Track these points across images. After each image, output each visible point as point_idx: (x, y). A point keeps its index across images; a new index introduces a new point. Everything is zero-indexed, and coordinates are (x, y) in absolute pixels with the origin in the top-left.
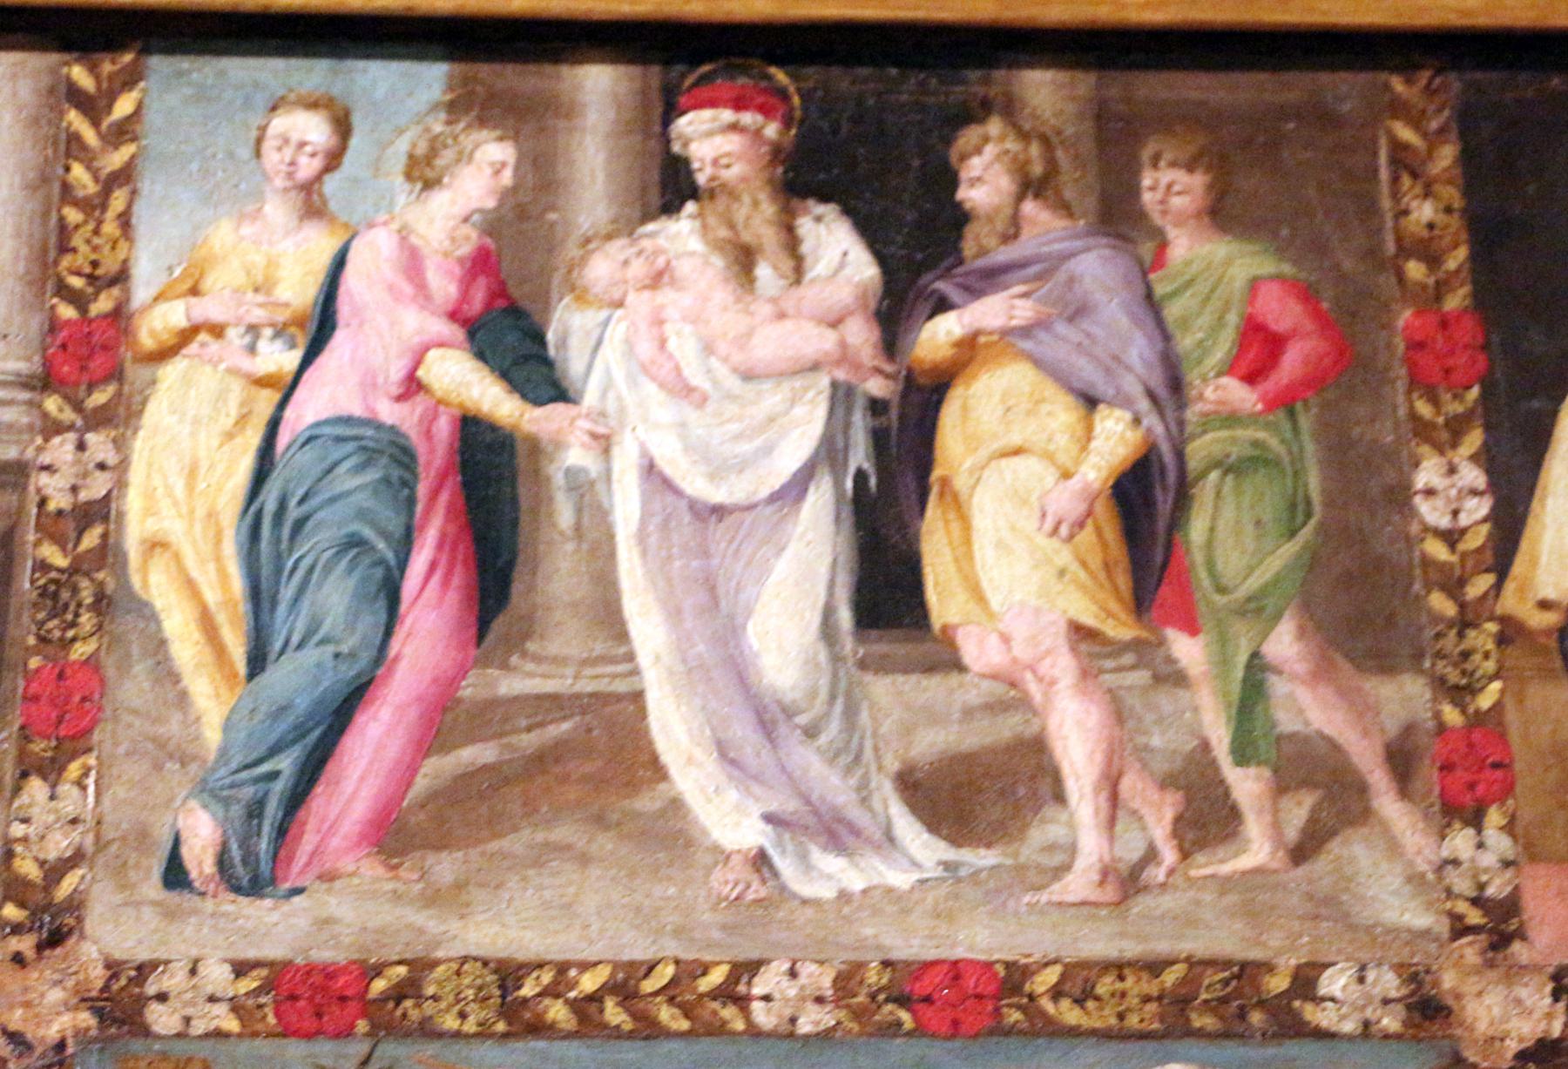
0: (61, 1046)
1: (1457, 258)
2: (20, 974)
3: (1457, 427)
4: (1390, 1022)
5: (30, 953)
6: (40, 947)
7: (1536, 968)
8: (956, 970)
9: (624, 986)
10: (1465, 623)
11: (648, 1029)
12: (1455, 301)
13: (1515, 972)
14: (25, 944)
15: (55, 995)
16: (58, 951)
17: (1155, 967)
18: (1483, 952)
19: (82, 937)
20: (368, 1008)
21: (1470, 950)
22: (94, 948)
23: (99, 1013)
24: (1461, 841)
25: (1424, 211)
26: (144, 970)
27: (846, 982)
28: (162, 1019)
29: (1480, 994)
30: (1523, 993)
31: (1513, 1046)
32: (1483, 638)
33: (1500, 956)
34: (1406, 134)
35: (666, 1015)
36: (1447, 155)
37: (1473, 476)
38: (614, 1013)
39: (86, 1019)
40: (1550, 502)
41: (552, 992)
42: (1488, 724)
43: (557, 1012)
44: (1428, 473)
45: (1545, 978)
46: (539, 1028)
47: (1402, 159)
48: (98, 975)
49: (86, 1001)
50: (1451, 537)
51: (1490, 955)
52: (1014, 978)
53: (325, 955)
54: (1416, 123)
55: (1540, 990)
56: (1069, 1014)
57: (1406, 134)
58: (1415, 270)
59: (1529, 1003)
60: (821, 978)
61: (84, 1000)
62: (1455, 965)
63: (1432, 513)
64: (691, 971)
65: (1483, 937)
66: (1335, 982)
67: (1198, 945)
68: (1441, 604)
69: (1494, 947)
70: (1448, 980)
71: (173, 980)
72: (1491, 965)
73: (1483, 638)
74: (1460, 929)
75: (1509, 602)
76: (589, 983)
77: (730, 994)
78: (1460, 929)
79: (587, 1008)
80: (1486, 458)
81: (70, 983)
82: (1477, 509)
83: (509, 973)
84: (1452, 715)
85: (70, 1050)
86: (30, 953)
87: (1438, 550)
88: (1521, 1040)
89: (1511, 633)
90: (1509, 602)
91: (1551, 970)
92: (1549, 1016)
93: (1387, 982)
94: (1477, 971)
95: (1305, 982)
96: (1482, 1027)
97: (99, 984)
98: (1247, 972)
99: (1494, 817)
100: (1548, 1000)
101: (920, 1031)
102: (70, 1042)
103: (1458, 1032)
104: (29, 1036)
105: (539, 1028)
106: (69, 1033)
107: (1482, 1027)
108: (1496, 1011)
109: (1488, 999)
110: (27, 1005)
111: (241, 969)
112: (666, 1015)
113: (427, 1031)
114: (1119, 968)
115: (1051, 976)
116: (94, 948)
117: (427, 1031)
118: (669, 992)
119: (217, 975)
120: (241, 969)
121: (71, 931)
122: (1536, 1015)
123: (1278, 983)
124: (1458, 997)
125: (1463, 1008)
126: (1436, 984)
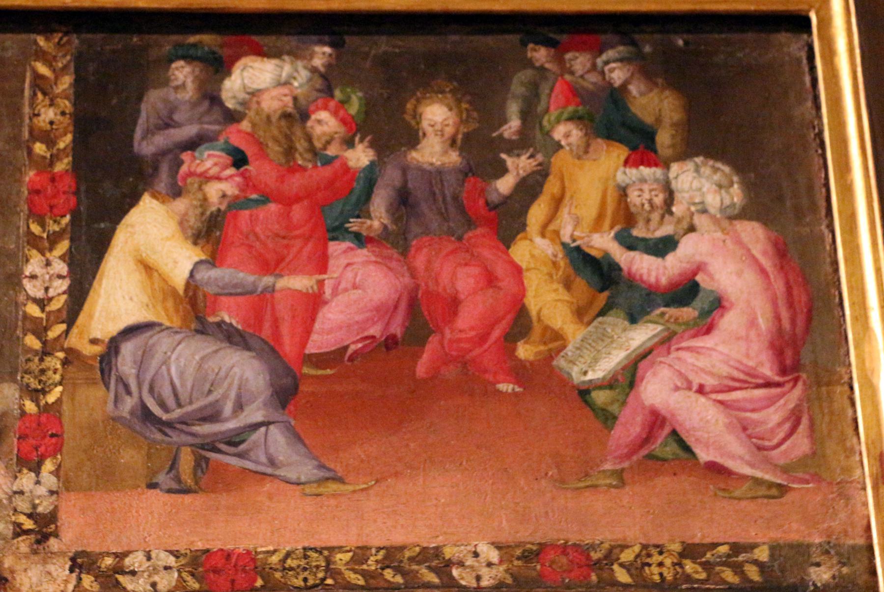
1: (65, 141)
3: (54, 240)
7: (62, 554)
10: (45, 353)
12: (61, 166)
21: (23, 545)
24: (26, 480)
25: (48, 114)
29: (25, 570)
30: (51, 568)
32: (54, 362)
33: (41, 547)
34: (42, 69)
36: (66, 81)
37: (61, 267)
40: (104, 282)
42: (52, 411)
44: (34, 265)
45: (67, 559)
47: (40, 84)
50: (41, 303)
51: (35, 546)
54: (49, 64)
55: (62, 567)
57: (42, 69)
58: (39, 148)
59: (54, 574)
62: (13, 553)
63: (33, 289)
65: (32, 537)
68: (32, 342)
69: (38, 542)
72: (35, 552)
73: (54, 362)
74: (19, 531)
75: (73, 341)
78: (19, 531)
80: (69, 258)
82: (62, 285)
84: (30, 407)
87: (33, 310)
89: (72, 358)
90: (73, 341)
91: (71, 554)
94: (26, 557)
99: (48, 466)
100: (67, 572)
108: (34, 580)
109: (30, 574)
122: (59, 581)
124: (12, 572)
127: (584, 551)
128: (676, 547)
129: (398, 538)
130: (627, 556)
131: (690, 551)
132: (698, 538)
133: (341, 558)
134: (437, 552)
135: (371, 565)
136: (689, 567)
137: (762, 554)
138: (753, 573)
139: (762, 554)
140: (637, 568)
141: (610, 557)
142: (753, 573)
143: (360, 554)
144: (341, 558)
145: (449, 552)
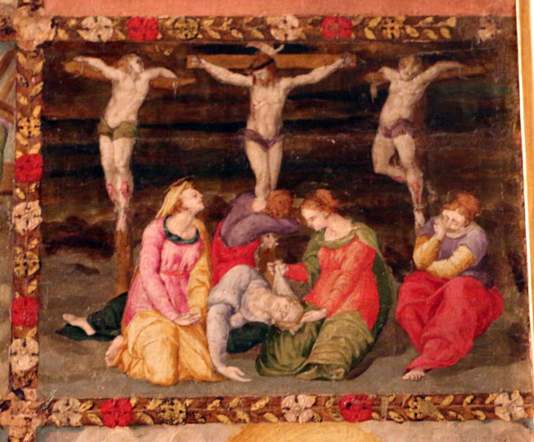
7: (46, 17)
13: (39, 19)
18: (29, 12)
21: (24, 11)
29: (26, 26)
31: (36, 43)
33: (34, 13)
45: (49, 20)
51: (31, 13)
59: (42, 29)
62: (18, 16)
65: (29, 7)
70: (16, 21)
72: (31, 16)
88: (39, 41)
91: (51, 18)
92: (49, 33)
94: (26, 18)
96: (26, 37)
100: (49, 28)
103: (17, 39)
107: (26, 37)
108: (31, 32)
109: (28, 28)
122: (45, 33)
124: (19, 27)
125: (19, 30)
126: (11, 22)
127: (347, 20)
128: (402, 18)
129: (240, 12)
130: (373, 24)
131: (410, 21)
132: (415, 14)
133: (207, 23)
134: (263, 20)
135: (225, 27)
136: (409, 30)
137: (452, 23)
138: (446, 34)
139: (452, 23)
140: (378, 30)
141: (363, 24)
142: (446, 34)
143: (218, 21)
144: (207, 23)
145: (270, 20)
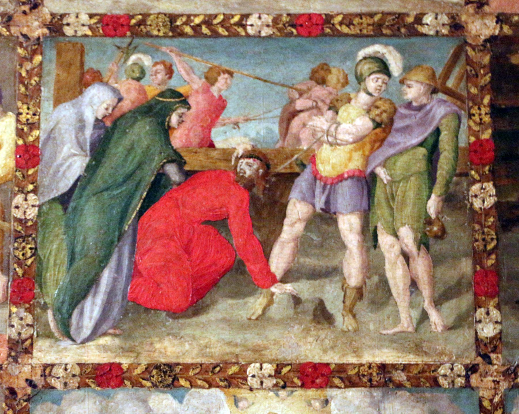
0: (39, 39)
2: (25, 17)
4: (445, 31)
5: (28, 11)
6: (31, 9)
8: (310, 16)
9: (208, 22)
11: (215, 35)
13: (484, 15)
14: (26, 8)
15: (36, 23)
16: (36, 10)
17: (371, 15)
19: (44, 6)
20: (130, 28)
22: (47, 10)
23: (49, 29)
26: (62, 16)
27: (276, 20)
28: (68, 31)
35: (221, 30)
38: (205, 30)
39: (46, 31)
41: (186, 23)
43: (188, 30)
46: (182, 34)
48: (48, 17)
49: (45, 25)
52: (328, 19)
53: (117, 12)
56: (345, 29)
60: (268, 19)
61: (45, 25)
64: (227, 17)
66: (428, 19)
67: (385, 8)
71: (71, 19)
76: (197, 21)
77: (241, 24)
79: (196, 28)
81: (40, 20)
83: (172, 18)
85: (41, 40)
86: (28, 11)
93: (444, 19)
95: (419, 19)
97: (49, 20)
98: (400, 16)
101: (299, 35)
102: (41, 37)
104: (29, 36)
105: (182, 34)
106: (41, 35)
110: (28, 26)
111: (91, 16)
112: (221, 30)
113: (148, 35)
114: (360, 15)
115: (340, 18)
116: (47, 10)
117: (148, 35)
118: (222, 24)
119: (84, 18)
120: (91, 16)
121: (40, 4)
123: (410, 20)
